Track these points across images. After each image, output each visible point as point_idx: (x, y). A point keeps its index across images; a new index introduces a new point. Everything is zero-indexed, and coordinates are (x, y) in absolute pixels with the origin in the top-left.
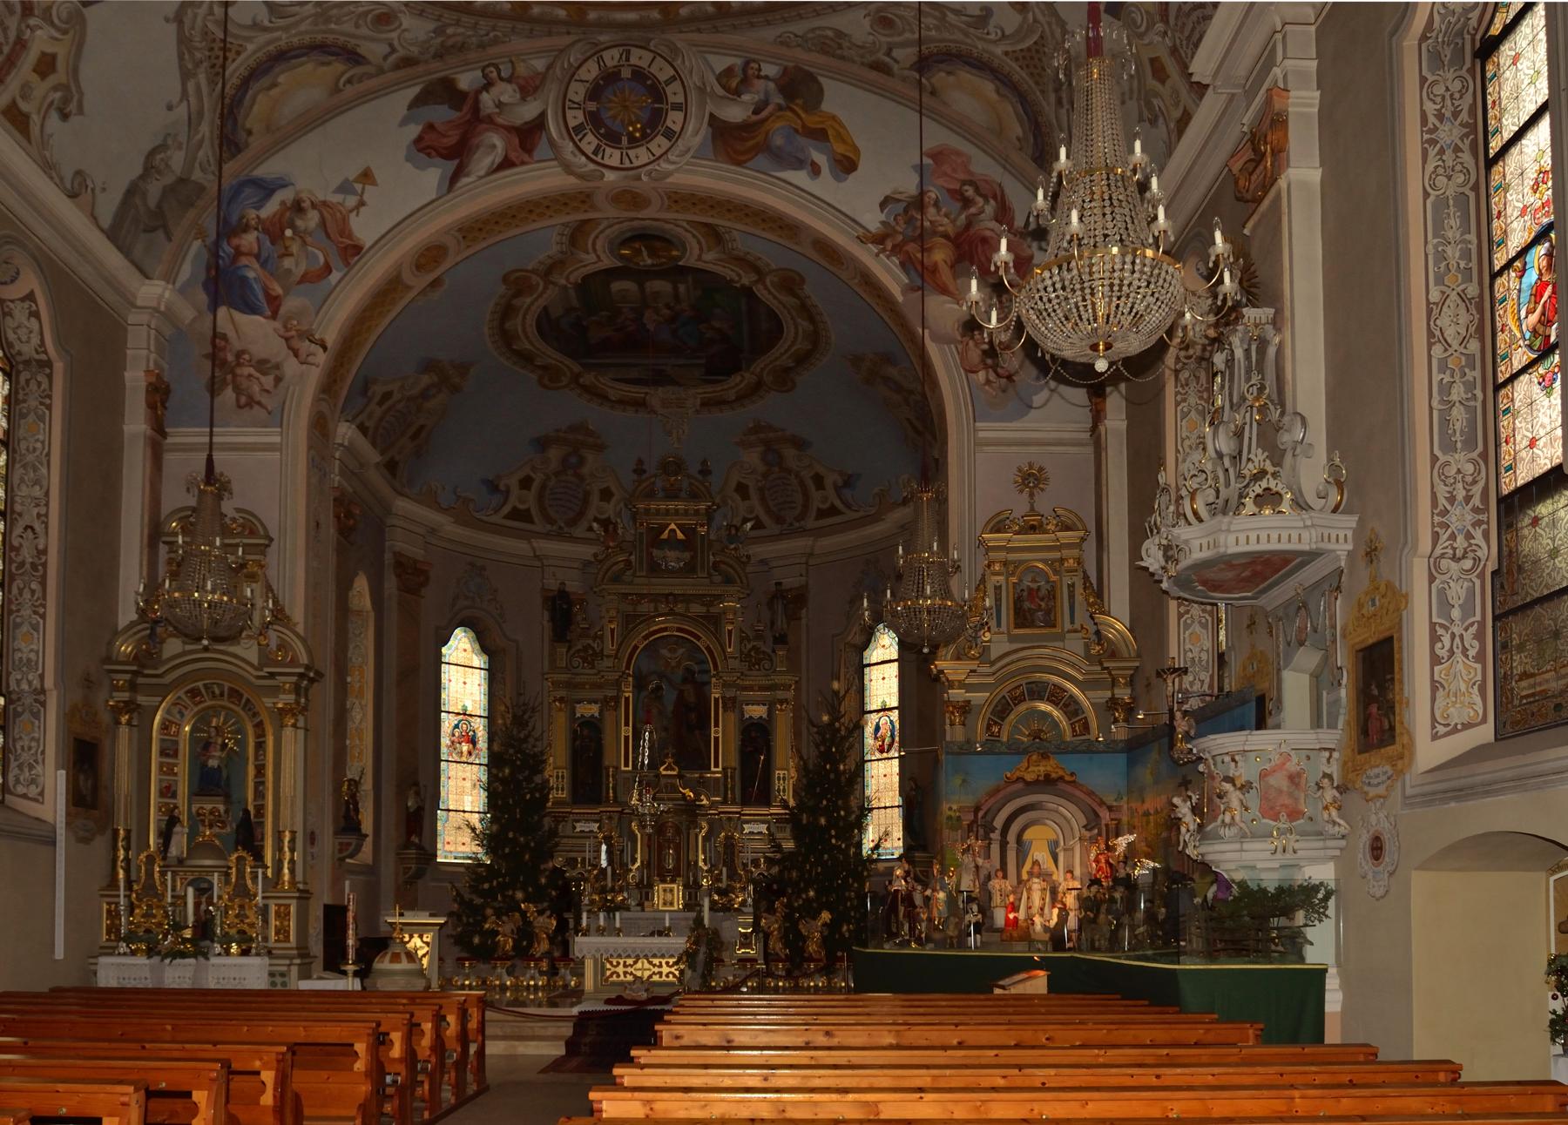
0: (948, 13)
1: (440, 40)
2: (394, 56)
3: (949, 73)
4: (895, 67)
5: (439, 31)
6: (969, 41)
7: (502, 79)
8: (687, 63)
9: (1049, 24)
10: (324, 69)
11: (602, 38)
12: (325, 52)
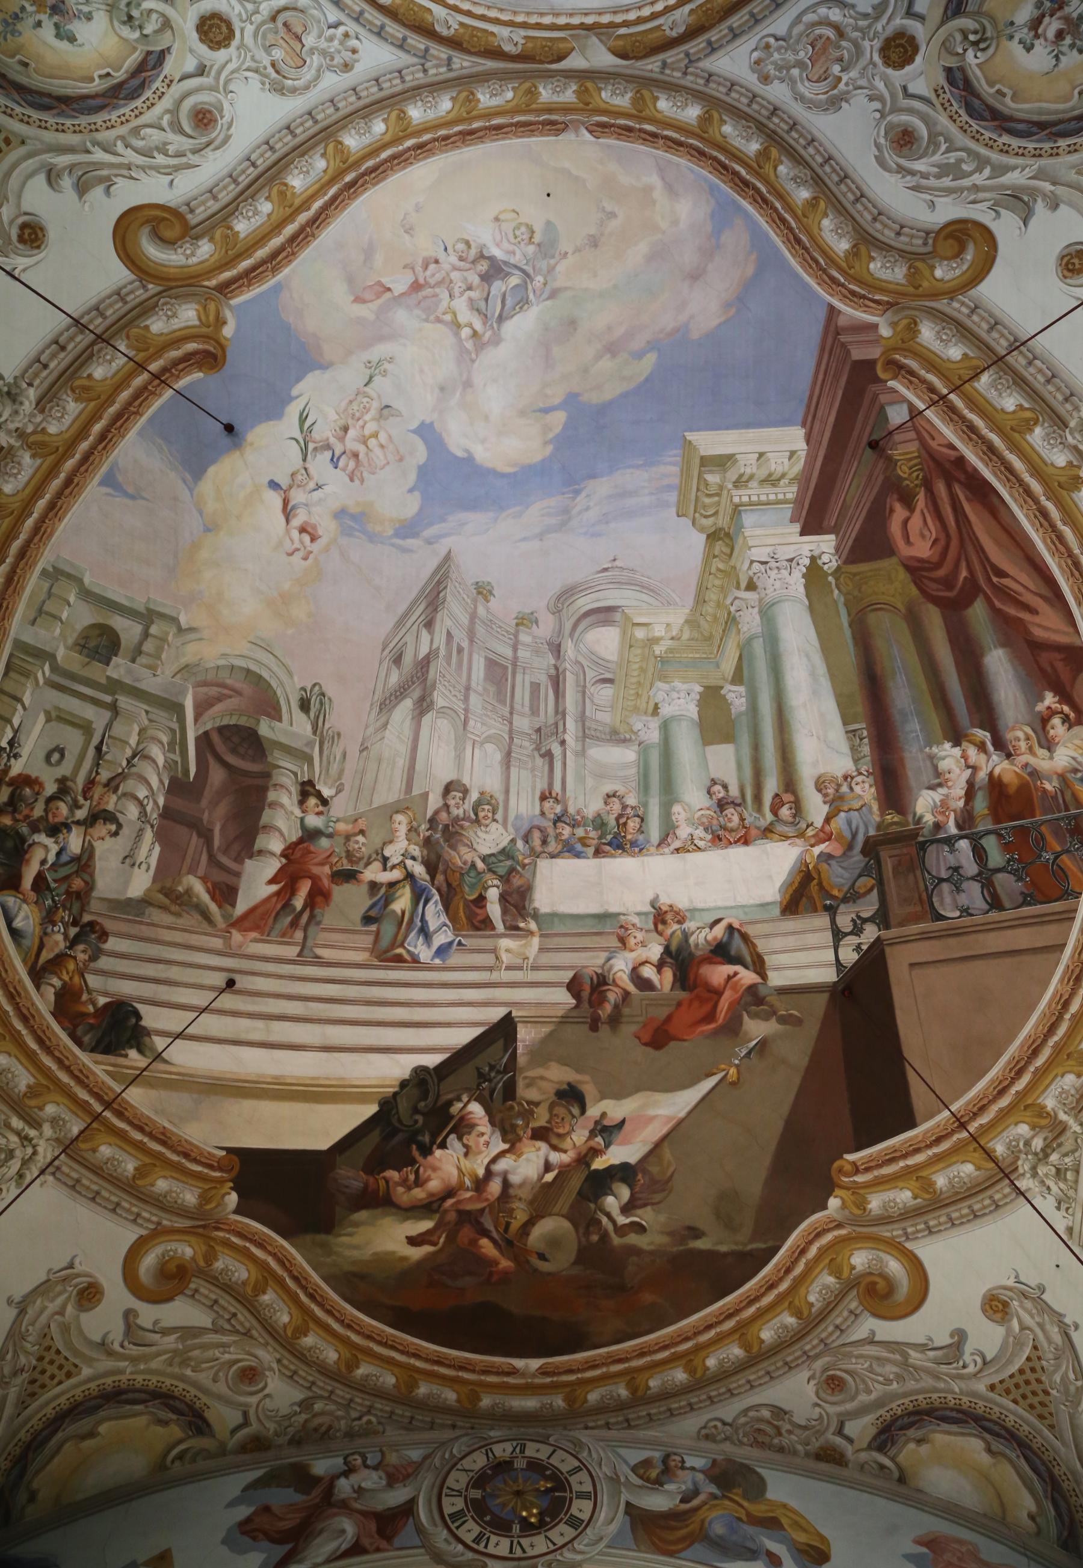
0: (912, 1353)
1: (304, 1416)
2: (246, 1431)
3: (919, 1441)
4: (849, 1450)
5: (305, 1405)
6: (942, 1385)
7: (367, 1467)
8: (594, 1455)
9: (1041, 1326)
10: (159, 1429)
11: (492, 1433)
12: (166, 1405)
